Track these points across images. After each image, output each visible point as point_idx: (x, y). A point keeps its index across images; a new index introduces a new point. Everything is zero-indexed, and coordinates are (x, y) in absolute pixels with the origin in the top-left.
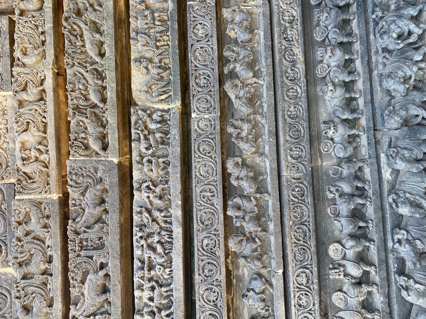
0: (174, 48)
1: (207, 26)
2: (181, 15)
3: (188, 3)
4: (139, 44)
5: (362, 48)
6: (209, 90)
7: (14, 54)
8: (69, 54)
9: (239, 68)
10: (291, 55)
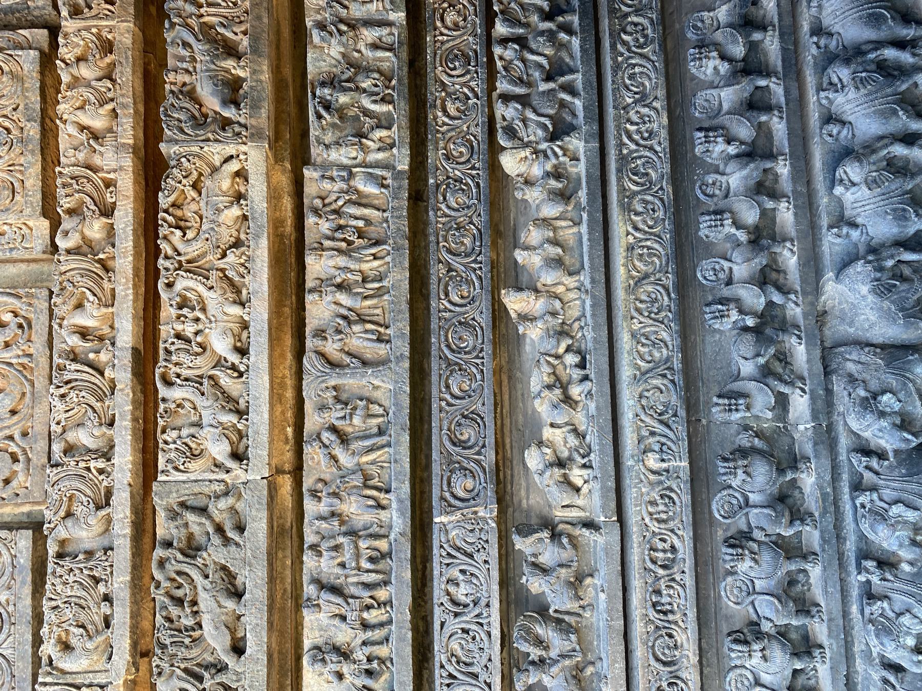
0: (401, 628)
1: (477, 577)
2: (418, 480)
3: (436, 520)
4: (322, 614)
5: (834, 646)
7: (41, 649)
8: (163, 647)
9: (546, 680)
10: (669, 648)
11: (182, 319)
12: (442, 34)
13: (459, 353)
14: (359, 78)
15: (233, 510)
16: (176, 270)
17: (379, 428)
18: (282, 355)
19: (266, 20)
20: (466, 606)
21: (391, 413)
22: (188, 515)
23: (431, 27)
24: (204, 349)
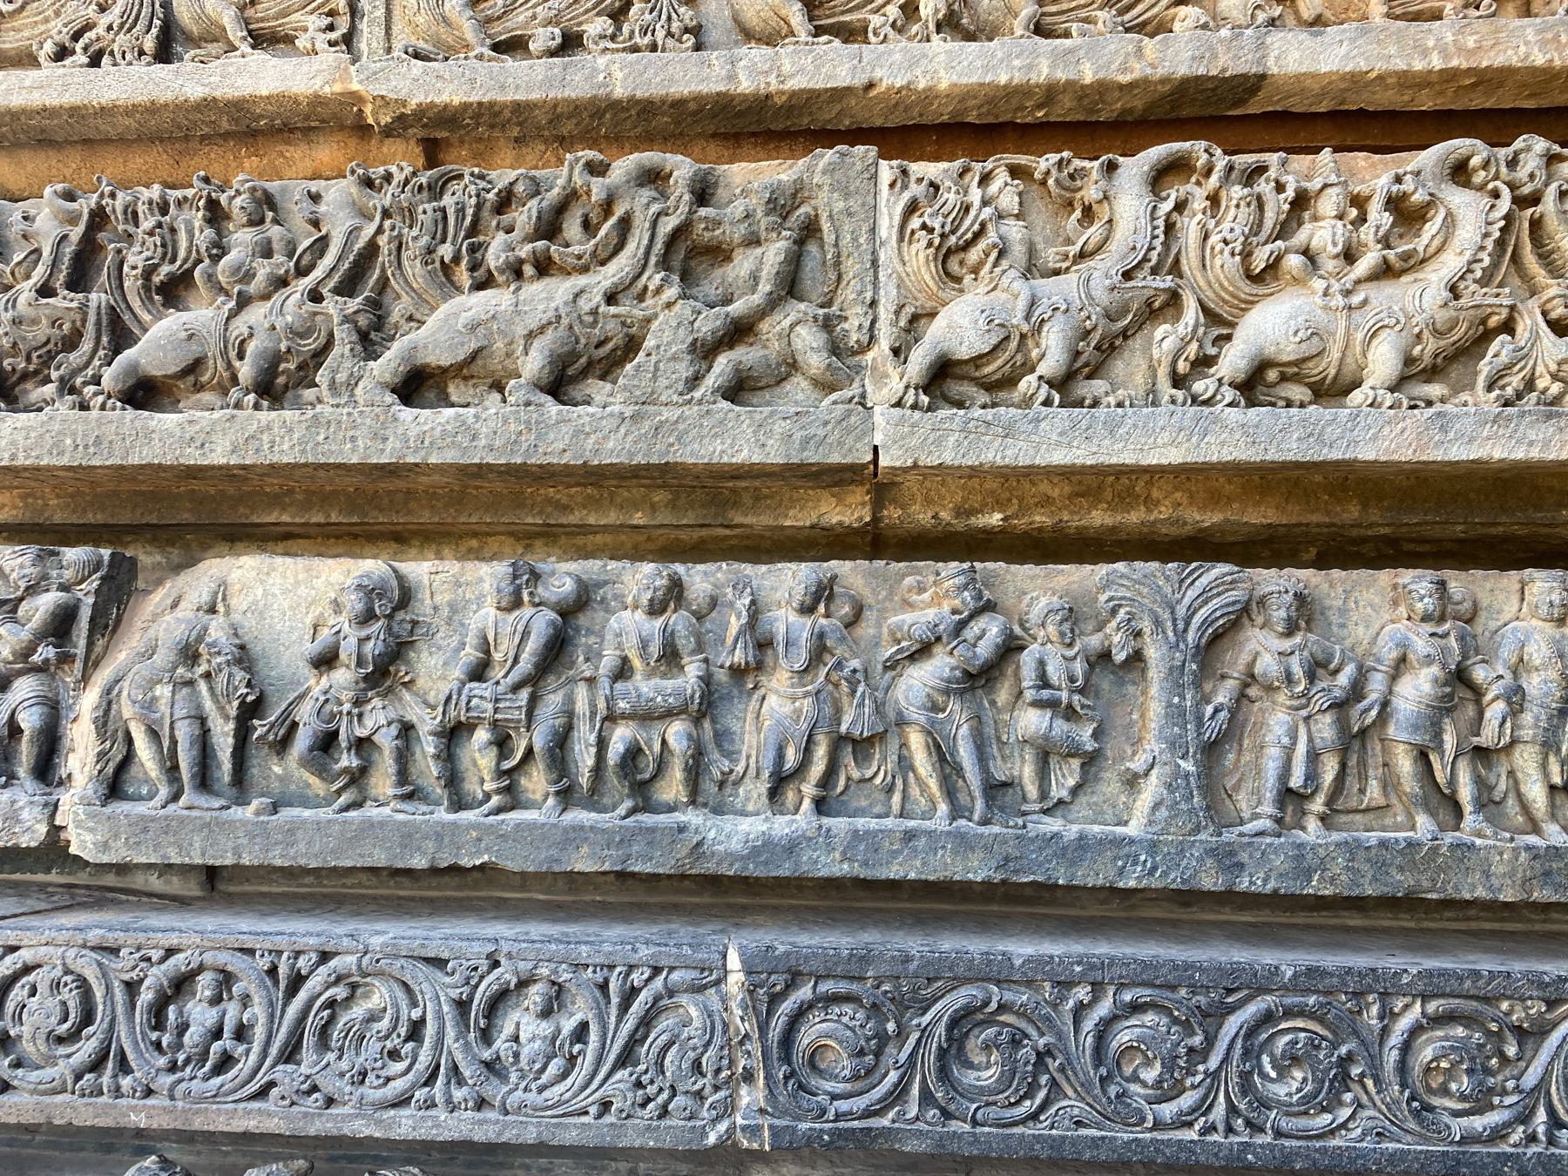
0: (439, 837)
1: (564, 1076)
4: (493, 611)
6: (130, 1056)
8: (435, 190)
11: (1354, 212)
13: (1246, 1053)
15: (792, 365)
16: (1512, 186)
17: (1005, 785)
18: (1215, 499)
20: (486, 1037)
21: (1052, 825)
22: (782, 244)
24: (1256, 279)
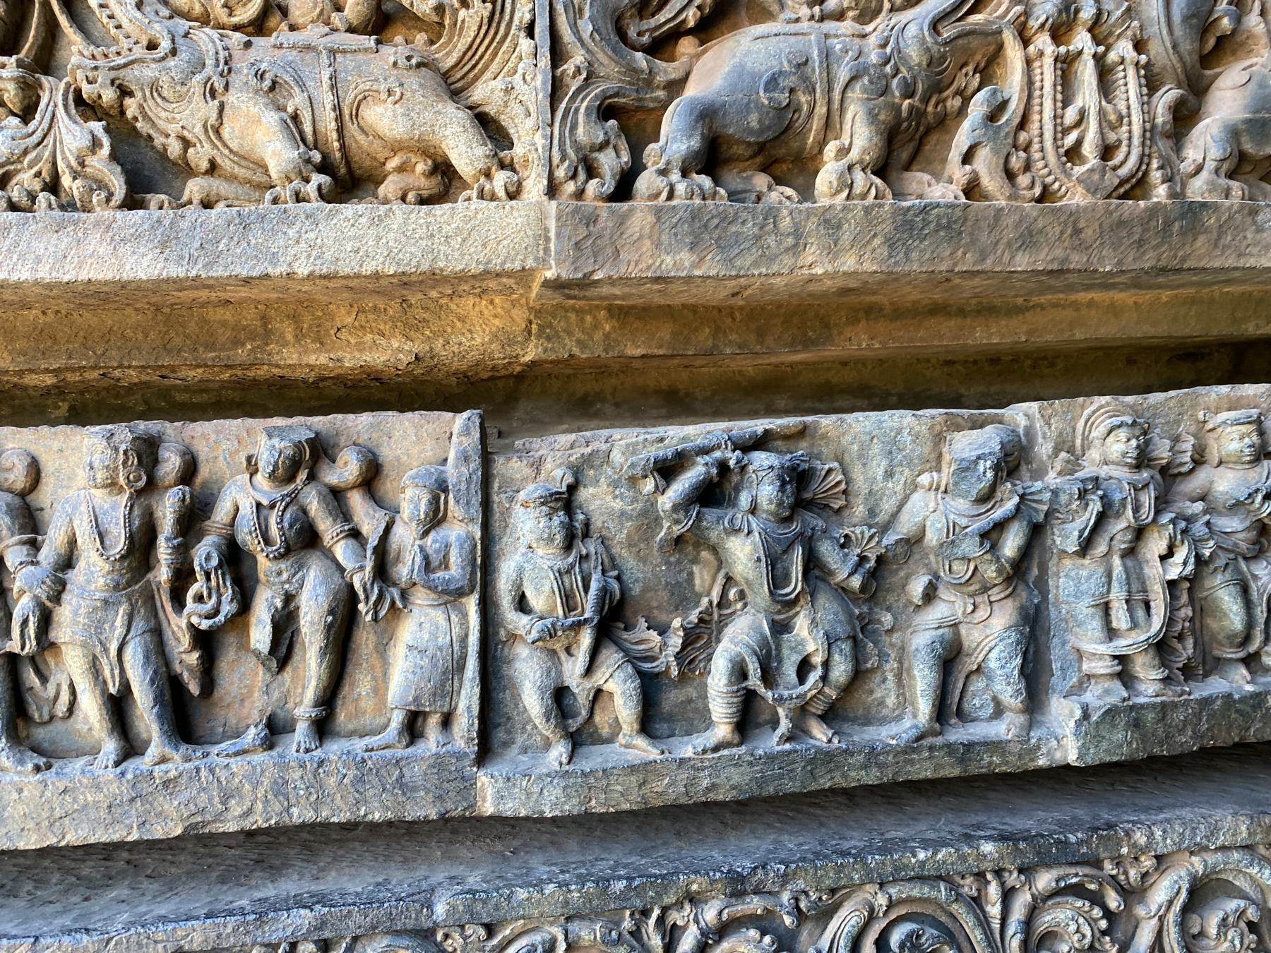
12: (1007, 895)
14: (828, 608)
19: (1022, 262)
23: (1031, 857)
